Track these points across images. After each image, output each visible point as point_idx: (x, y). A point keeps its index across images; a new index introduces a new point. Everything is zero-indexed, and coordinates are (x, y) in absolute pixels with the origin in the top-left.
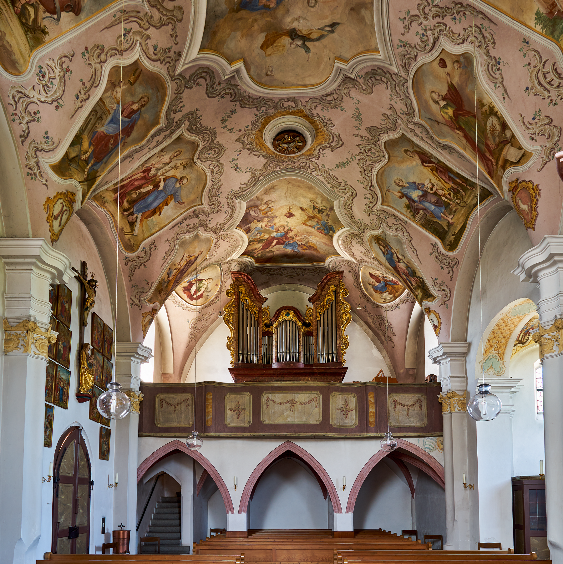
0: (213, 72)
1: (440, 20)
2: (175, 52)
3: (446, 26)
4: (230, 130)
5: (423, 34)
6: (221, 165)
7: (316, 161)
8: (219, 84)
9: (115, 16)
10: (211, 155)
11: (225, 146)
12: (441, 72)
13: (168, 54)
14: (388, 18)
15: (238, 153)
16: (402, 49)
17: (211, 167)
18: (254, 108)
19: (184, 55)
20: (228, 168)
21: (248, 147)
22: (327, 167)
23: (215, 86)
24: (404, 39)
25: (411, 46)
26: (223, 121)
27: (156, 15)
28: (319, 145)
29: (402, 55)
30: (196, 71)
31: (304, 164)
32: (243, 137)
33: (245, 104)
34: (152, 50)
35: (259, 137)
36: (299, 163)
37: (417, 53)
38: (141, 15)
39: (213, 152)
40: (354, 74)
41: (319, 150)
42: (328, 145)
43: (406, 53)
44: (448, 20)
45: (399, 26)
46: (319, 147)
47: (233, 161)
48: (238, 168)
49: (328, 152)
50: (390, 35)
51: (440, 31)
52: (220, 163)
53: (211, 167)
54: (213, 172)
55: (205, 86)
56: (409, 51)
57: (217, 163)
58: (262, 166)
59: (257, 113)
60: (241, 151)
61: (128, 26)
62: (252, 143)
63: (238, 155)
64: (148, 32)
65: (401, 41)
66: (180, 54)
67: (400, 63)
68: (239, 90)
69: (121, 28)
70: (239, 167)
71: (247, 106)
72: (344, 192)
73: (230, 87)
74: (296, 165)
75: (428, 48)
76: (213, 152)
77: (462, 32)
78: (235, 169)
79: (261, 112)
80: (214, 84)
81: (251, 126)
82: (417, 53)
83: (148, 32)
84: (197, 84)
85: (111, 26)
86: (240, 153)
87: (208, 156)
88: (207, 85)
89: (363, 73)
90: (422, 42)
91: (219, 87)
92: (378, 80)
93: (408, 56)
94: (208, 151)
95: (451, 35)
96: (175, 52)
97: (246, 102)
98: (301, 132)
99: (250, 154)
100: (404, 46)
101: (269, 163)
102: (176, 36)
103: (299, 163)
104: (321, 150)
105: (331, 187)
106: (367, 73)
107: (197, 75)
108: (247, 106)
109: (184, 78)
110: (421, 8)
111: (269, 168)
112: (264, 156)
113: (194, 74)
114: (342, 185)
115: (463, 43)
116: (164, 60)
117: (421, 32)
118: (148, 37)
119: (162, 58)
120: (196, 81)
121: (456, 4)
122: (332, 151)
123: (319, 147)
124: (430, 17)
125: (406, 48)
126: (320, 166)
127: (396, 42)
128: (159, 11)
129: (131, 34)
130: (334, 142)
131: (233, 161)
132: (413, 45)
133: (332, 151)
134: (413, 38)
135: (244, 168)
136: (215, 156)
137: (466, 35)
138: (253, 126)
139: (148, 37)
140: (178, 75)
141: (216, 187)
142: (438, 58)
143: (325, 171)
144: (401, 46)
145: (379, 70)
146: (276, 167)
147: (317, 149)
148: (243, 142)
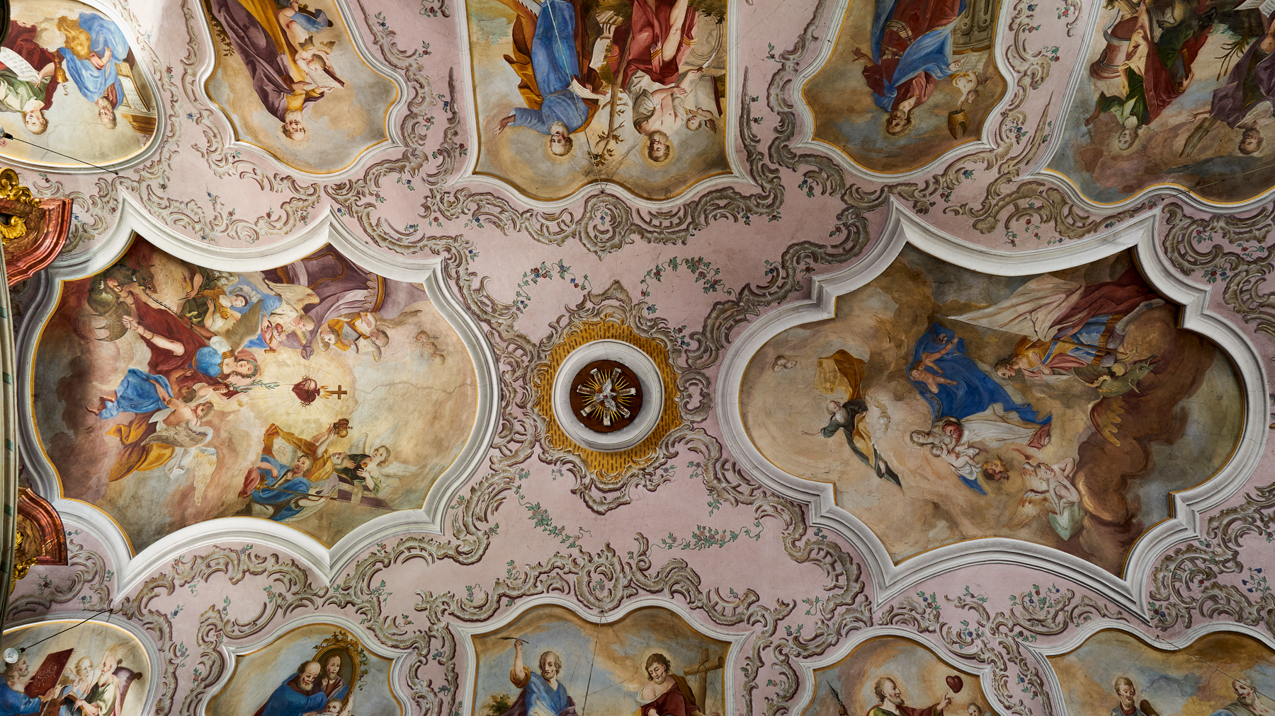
0: (841, 262)
1: (1006, 657)
2: (933, 204)
3: (1006, 669)
4: (658, 274)
5: (970, 634)
6: (560, 238)
7: (535, 457)
8: (808, 270)
9: (1050, 124)
10: (597, 221)
11: (607, 257)
12: (941, 689)
13: (940, 191)
14: (960, 567)
15: (579, 281)
16: (923, 604)
17: (566, 217)
18: (705, 327)
19: (917, 219)
20: (547, 254)
21: (589, 305)
22: (524, 482)
23: (810, 261)
24: (940, 601)
25: (937, 616)
26: (693, 264)
27: (1006, 189)
28: (584, 461)
29: (910, 604)
30: (867, 233)
31: (518, 427)
32: (620, 296)
33: (724, 311)
34: (968, 166)
35: (612, 331)
36: (521, 417)
37: (934, 631)
38: (1022, 165)
39: (602, 228)
40: (819, 520)
41: (570, 462)
42: (587, 481)
43: (920, 611)
44: (1013, 670)
45: (957, 592)
46: (577, 461)
47: (562, 267)
48: (538, 276)
49: (570, 481)
50: (933, 576)
51: (993, 661)
52: (567, 237)
53: (566, 217)
54: (550, 217)
55: (821, 243)
56: (926, 616)
57: (569, 231)
58: (523, 332)
59: (686, 332)
60: (583, 288)
61: (1024, 140)
62: (598, 314)
63: (573, 280)
64: (995, 169)
65: (934, 596)
66: (922, 211)
67: (896, 604)
68: (769, 303)
69: (1030, 128)
70: (540, 280)
71: (714, 315)
72: (459, 531)
73: (788, 287)
74: (517, 412)
75: (956, 648)
76: (607, 226)
77: (1015, 701)
78: (536, 271)
79: (687, 340)
80: (816, 260)
81: (652, 316)
82: (934, 631)
83: (995, 169)
84: (838, 229)
85: (1045, 114)
86: (576, 286)
87: (599, 214)
88: (821, 247)
89: (831, 537)
90: (959, 635)
91: (803, 266)
92: (834, 569)
93: (918, 617)
94: (613, 218)
95: (1001, 682)
96: (933, 204)
97: (729, 313)
98: (636, 421)
99: (568, 309)
100: (930, 605)
101: (529, 347)
102: (957, 213)
103: (521, 417)
104: (570, 466)
105: (462, 498)
106: (836, 546)
107: (858, 232)
108: (714, 315)
109: (871, 209)
110: (1001, 619)
111: (512, 347)
112: (550, 337)
113: (865, 227)
114: (478, 524)
115: (1008, 708)
116: (937, 182)
117: (973, 627)
118: (989, 167)
119: (942, 180)
120: (847, 227)
121: (1037, 675)
122: (574, 492)
123: (577, 461)
124: (998, 638)
125: (928, 610)
126: (521, 466)
127: (928, 589)
128: (1010, 195)
129: (1014, 140)
130: (602, 494)
131: (562, 267)
132: (941, 620)
133: (574, 492)
134: (955, 618)
135: (531, 290)
136: (590, 229)
137: (1018, 708)
138: (651, 320)
139: (989, 167)
140: (887, 199)
141: (503, 217)
142: (957, 673)
143: (512, 480)
144: (925, 600)
145: (855, 567)
146: (510, 364)
147: (570, 457)
148: (605, 296)
